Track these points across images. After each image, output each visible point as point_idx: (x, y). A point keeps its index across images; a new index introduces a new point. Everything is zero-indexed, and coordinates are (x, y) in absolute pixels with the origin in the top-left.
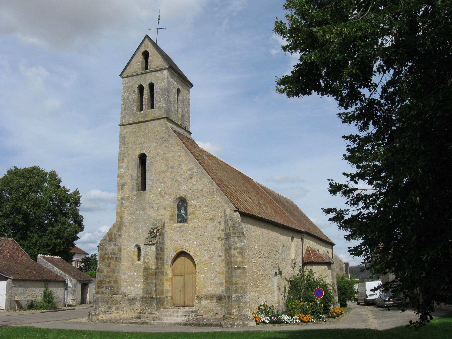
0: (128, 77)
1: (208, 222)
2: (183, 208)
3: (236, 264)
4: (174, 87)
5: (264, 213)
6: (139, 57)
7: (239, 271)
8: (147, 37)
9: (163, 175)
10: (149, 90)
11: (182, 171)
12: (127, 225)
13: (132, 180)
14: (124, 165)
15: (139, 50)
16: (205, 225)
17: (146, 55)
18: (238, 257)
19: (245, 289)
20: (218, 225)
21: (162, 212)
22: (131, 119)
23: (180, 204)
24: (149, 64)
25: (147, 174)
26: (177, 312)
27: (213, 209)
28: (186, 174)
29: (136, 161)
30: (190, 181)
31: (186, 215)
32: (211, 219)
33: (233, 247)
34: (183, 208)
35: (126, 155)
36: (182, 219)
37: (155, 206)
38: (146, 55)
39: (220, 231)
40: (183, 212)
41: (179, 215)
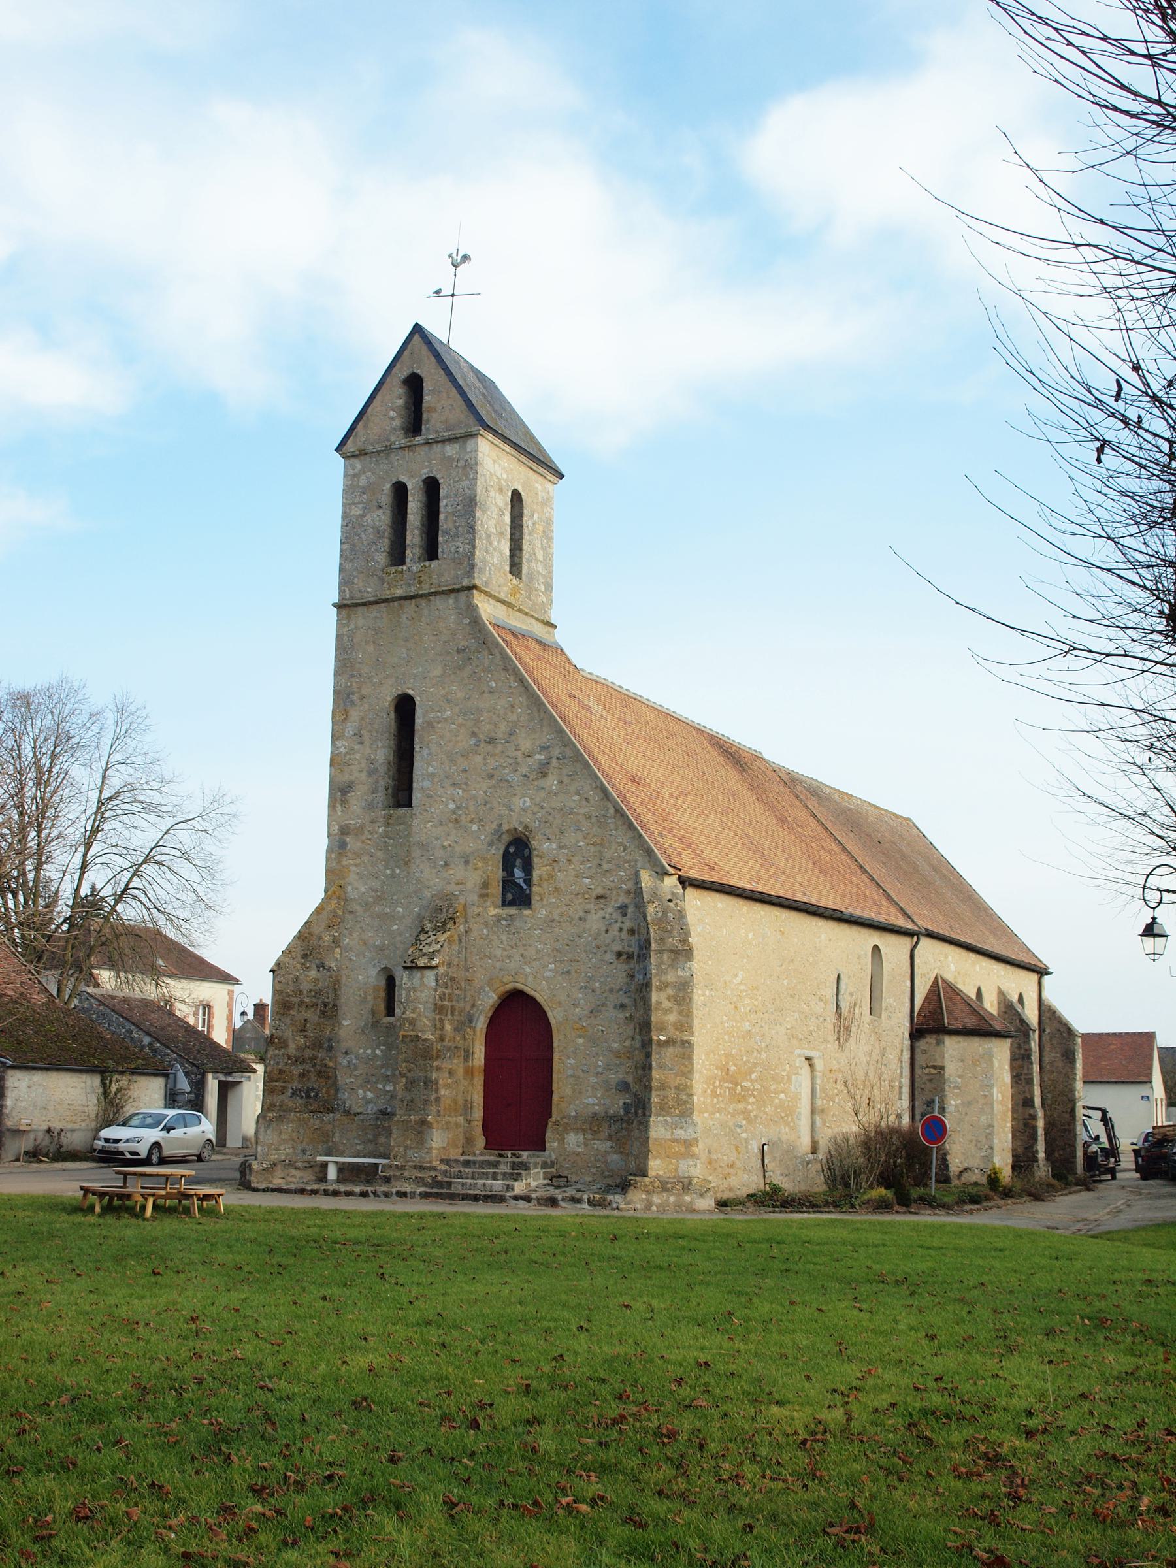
0: (361, 454)
1: (591, 906)
2: (518, 862)
3: (662, 1029)
4: (501, 490)
5: (774, 876)
6: (397, 397)
7: (670, 1051)
8: (417, 329)
9: (462, 763)
10: (424, 499)
11: (519, 754)
12: (358, 908)
13: (371, 773)
14: (350, 730)
15: (395, 370)
16: (581, 914)
17: (414, 384)
18: (670, 1010)
19: (686, 1102)
20: (617, 915)
21: (458, 871)
22: (370, 591)
23: (512, 850)
24: (425, 416)
25: (417, 764)
26: (495, 1165)
27: (606, 866)
28: (530, 761)
29: (387, 720)
30: (541, 783)
31: (528, 882)
32: (599, 897)
33: (655, 982)
34: (518, 862)
35: (355, 698)
36: (516, 895)
37: (439, 853)
38: (414, 384)
39: (624, 935)
40: (518, 873)
41: (508, 883)
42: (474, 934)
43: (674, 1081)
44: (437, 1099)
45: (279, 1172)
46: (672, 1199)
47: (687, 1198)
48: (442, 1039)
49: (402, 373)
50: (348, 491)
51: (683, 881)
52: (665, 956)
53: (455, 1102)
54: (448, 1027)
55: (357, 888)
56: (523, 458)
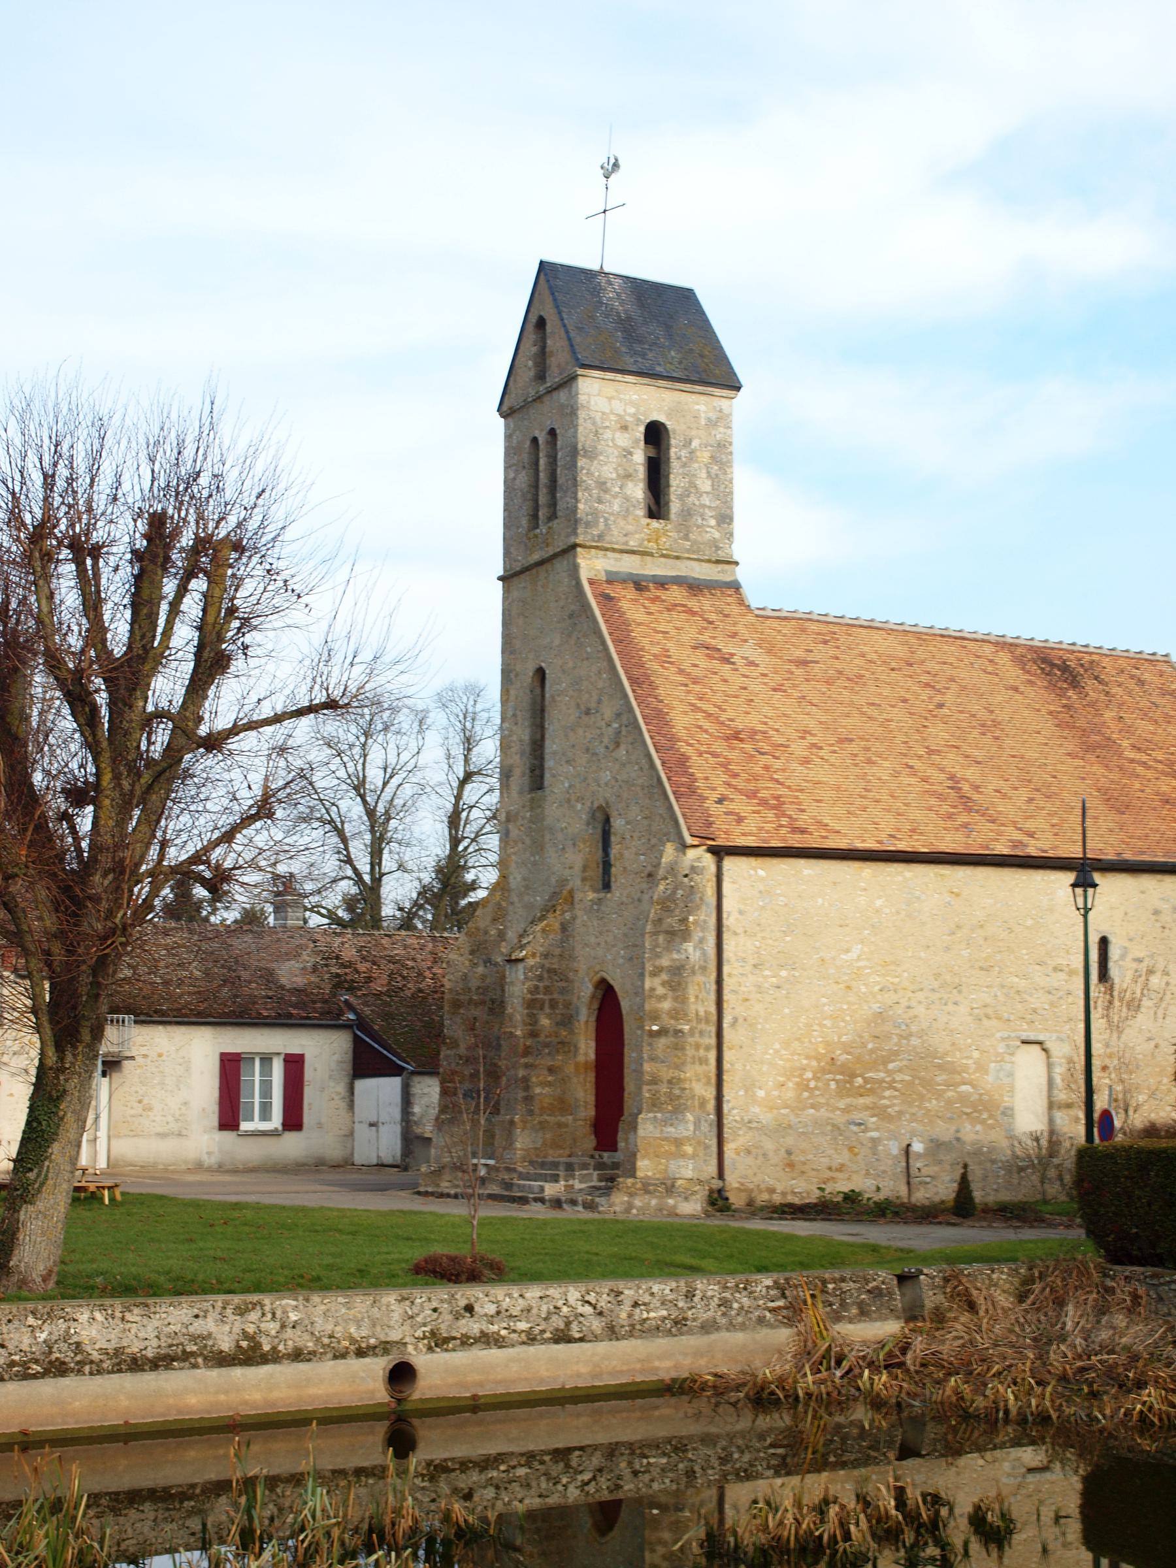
3: (655, 1018)
4: (625, 428)
7: (663, 1041)
18: (663, 998)
19: (679, 1097)
22: (522, 560)
28: (610, 729)
33: (649, 967)
42: (578, 921)
43: (666, 1073)
44: (528, 1099)
45: (447, 1176)
46: (654, 1202)
47: (671, 1201)
48: (533, 1034)
49: (533, 319)
50: (507, 454)
51: (719, 853)
52: (661, 939)
53: (562, 1100)
54: (545, 1022)
55: (516, 879)
56: (661, 383)
